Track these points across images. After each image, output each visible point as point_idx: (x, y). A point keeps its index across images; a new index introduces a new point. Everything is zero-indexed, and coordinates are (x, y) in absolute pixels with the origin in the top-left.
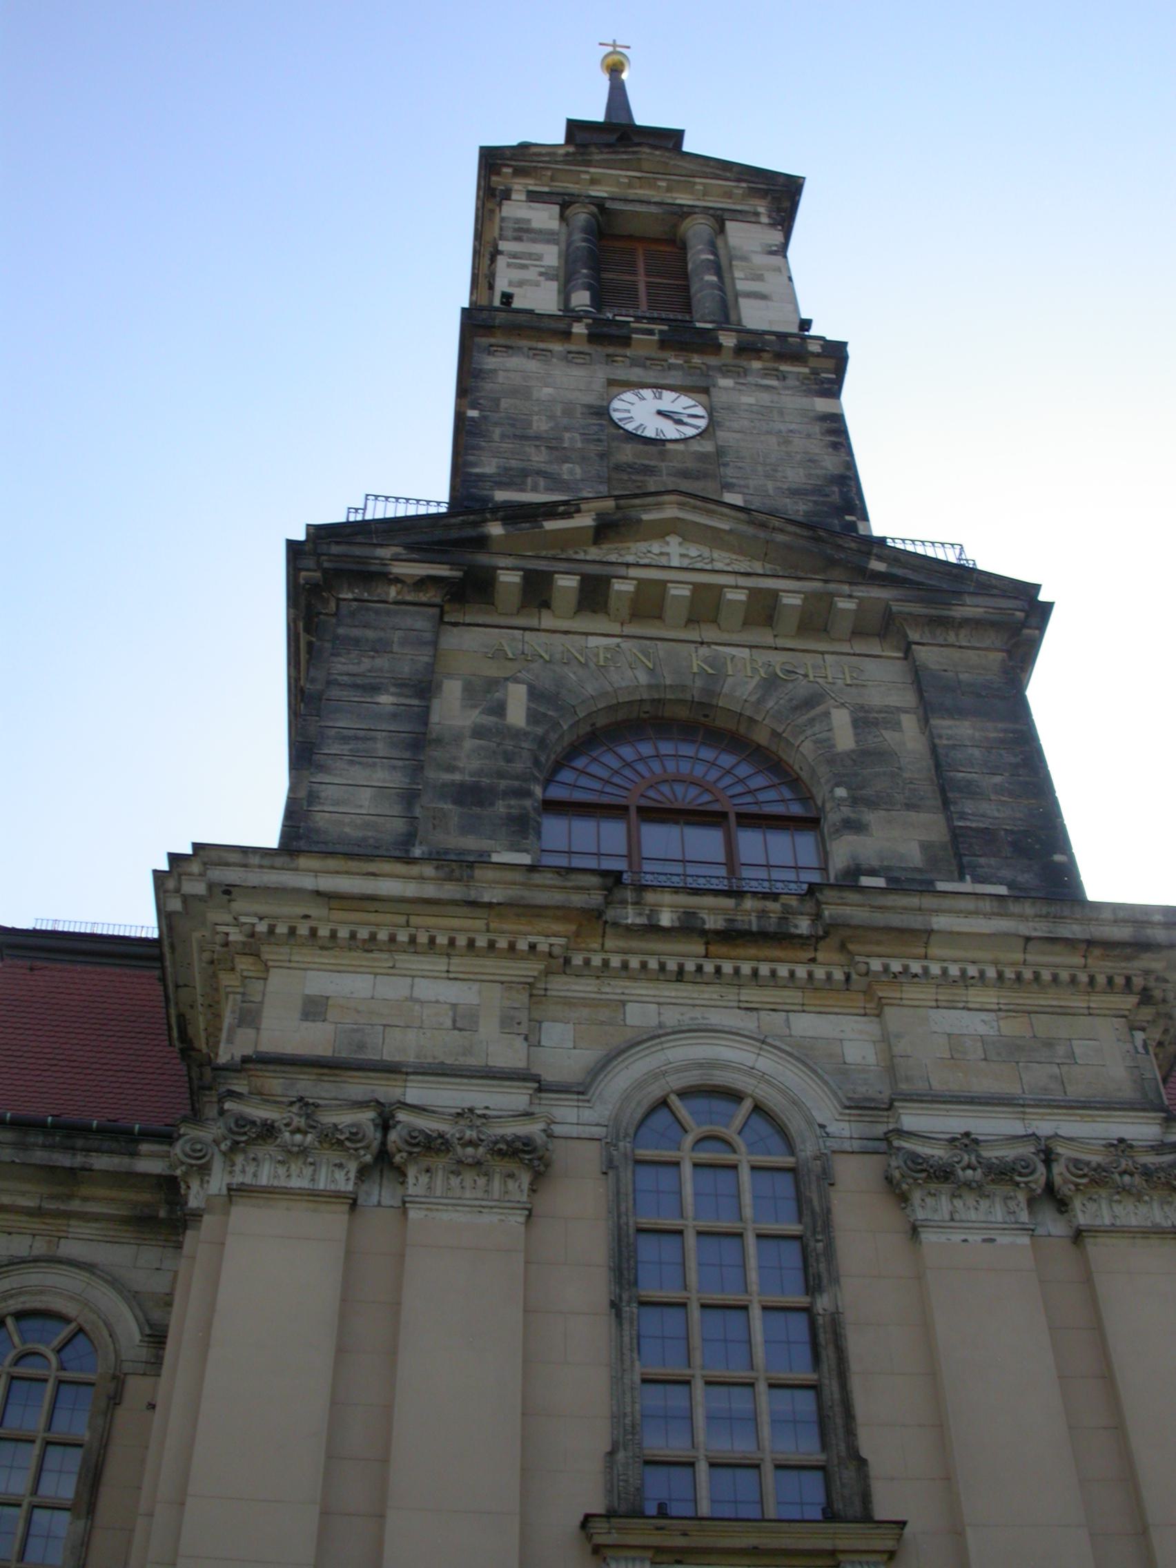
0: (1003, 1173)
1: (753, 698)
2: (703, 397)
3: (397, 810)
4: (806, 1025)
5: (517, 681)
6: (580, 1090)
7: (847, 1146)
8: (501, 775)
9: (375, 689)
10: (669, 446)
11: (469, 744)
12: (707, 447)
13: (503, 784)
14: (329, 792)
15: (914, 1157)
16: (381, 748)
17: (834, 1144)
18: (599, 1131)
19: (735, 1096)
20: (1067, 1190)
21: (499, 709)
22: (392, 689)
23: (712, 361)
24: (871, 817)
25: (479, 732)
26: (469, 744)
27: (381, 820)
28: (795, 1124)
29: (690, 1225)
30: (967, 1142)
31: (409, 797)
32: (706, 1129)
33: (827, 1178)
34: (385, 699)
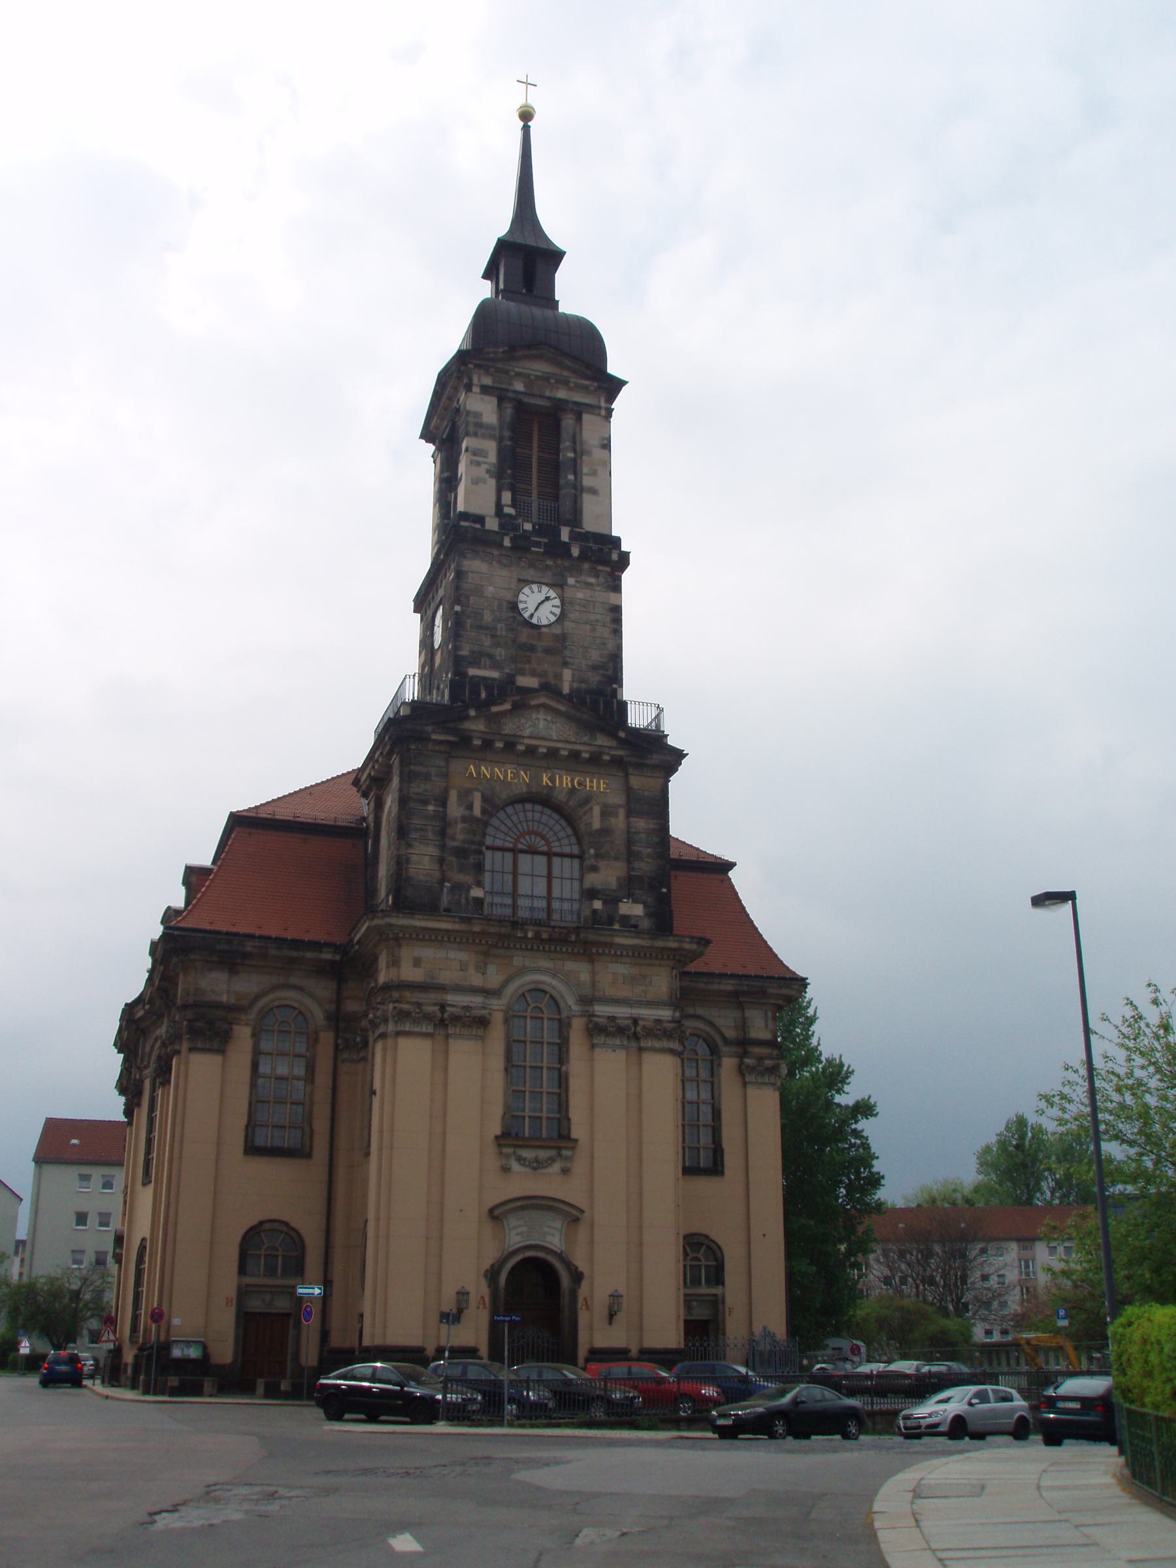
0: (621, 1031)
1: (565, 800)
2: (559, 590)
3: (437, 867)
4: (570, 965)
5: (478, 790)
6: (496, 993)
7: (577, 1014)
8: (472, 842)
9: (425, 802)
10: (543, 630)
11: (460, 826)
12: (557, 630)
13: (473, 847)
14: (414, 858)
15: (596, 1024)
16: (430, 835)
17: (573, 1013)
18: (503, 1008)
19: (545, 992)
20: (639, 1035)
21: (470, 807)
22: (433, 802)
23: (567, 564)
24: (601, 864)
25: (464, 819)
26: (460, 826)
27: (432, 872)
28: (562, 1005)
29: (529, 1039)
30: (612, 1019)
31: (441, 861)
32: (535, 1005)
33: (569, 1025)
34: (431, 808)
